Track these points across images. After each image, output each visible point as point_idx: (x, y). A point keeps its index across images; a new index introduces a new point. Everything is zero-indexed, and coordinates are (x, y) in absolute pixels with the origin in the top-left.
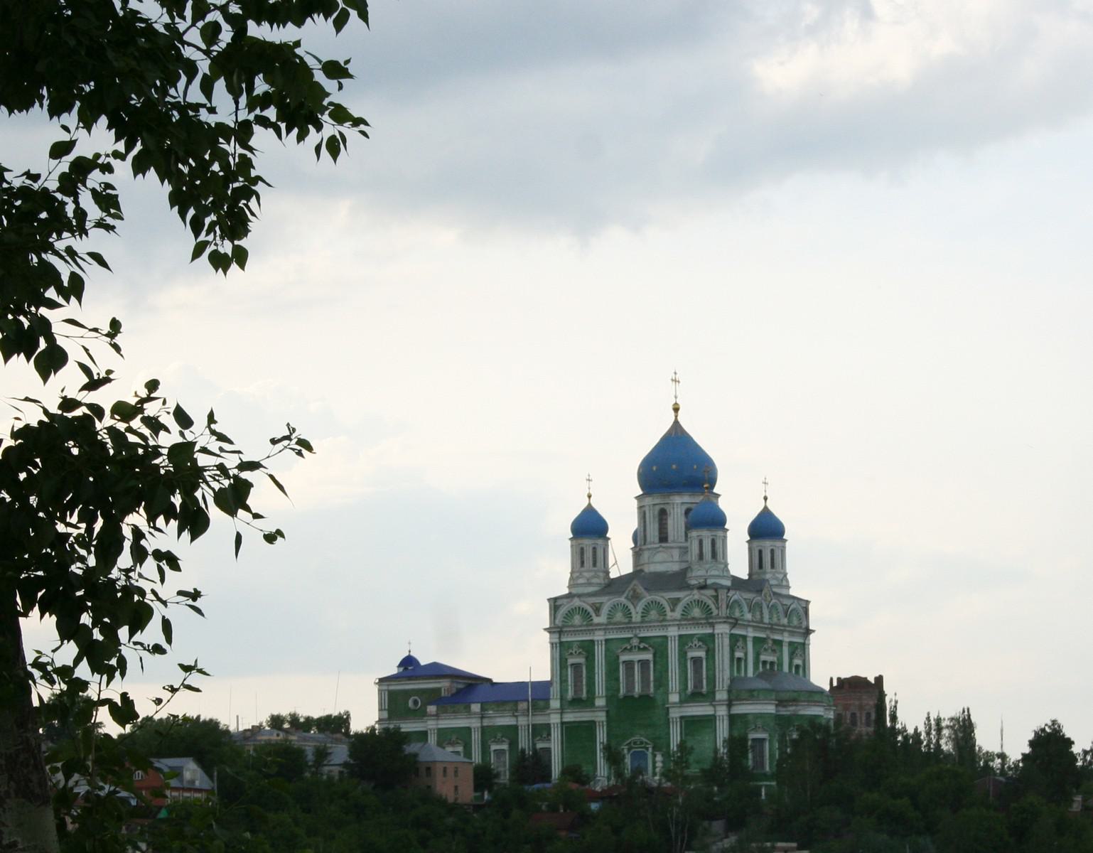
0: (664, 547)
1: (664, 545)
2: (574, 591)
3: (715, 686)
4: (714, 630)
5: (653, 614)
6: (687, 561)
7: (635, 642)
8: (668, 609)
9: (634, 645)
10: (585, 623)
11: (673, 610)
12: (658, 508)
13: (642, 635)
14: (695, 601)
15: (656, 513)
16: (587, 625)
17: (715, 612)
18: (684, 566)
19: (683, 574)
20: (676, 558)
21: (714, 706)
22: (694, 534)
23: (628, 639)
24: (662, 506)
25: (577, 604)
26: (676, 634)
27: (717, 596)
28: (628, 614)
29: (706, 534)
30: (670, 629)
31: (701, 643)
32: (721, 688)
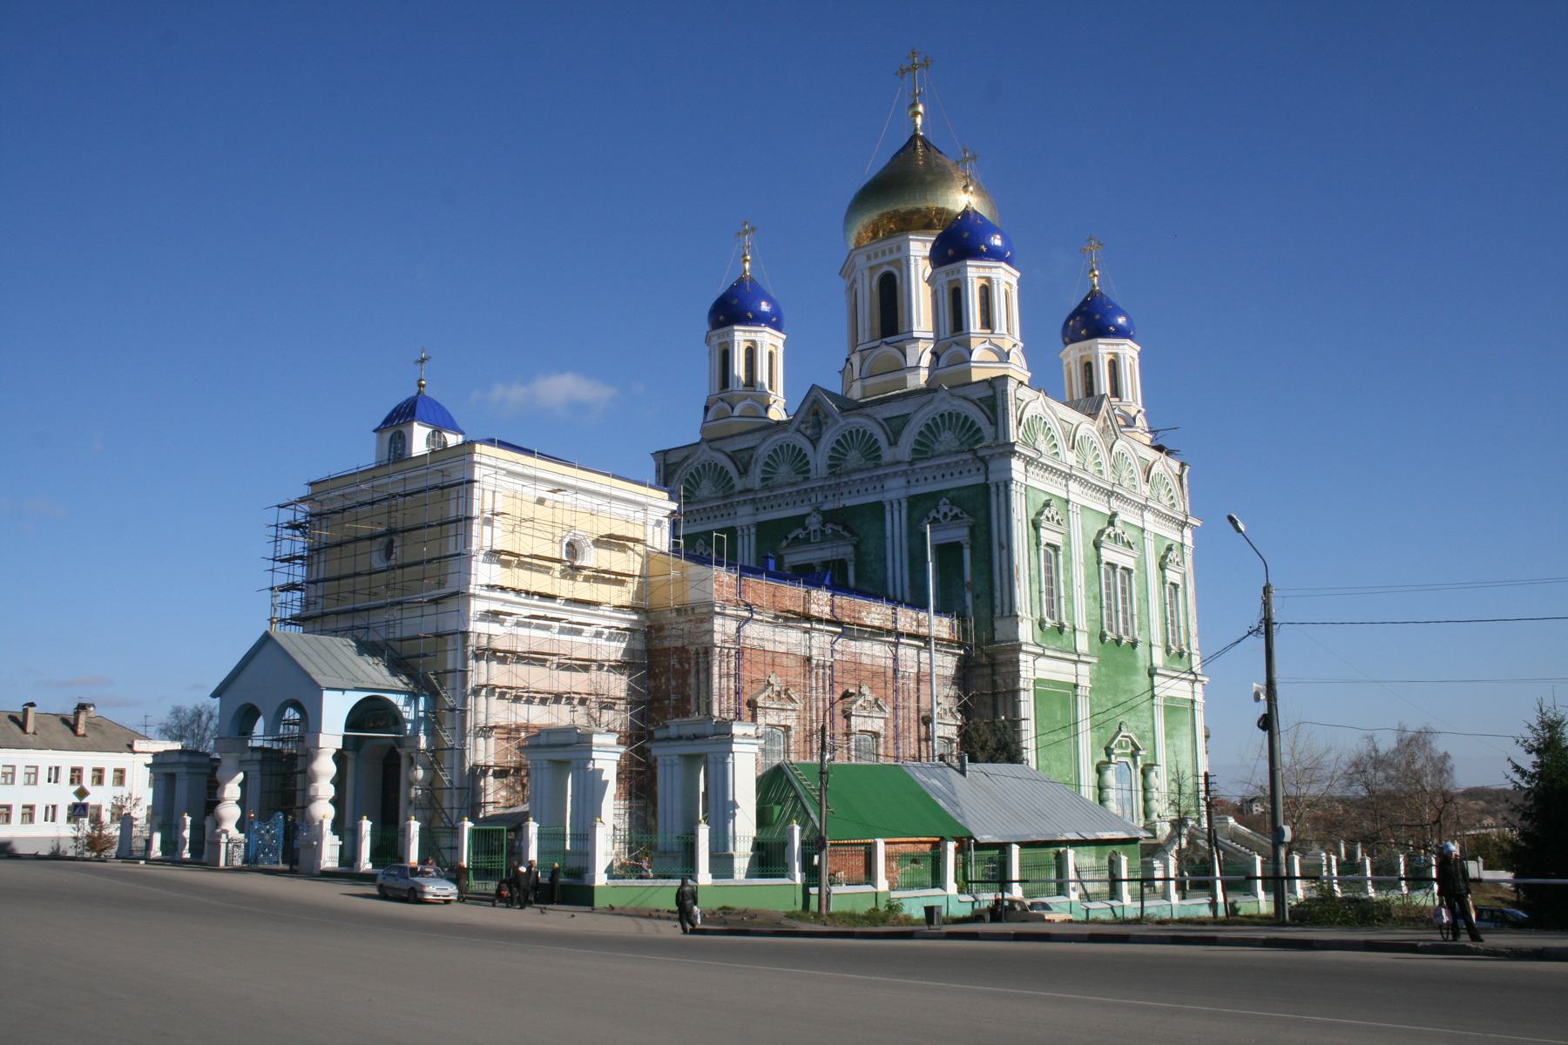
3: (993, 612)
5: (854, 457)
7: (814, 523)
9: (812, 528)
10: (720, 494)
11: (893, 443)
13: (826, 507)
14: (942, 415)
16: (724, 498)
23: (800, 521)
24: (886, 268)
25: (703, 459)
26: (902, 494)
27: (994, 397)
28: (800, 461)
30: (889, 484)
31: (956, 510)
32: (1006, 613)
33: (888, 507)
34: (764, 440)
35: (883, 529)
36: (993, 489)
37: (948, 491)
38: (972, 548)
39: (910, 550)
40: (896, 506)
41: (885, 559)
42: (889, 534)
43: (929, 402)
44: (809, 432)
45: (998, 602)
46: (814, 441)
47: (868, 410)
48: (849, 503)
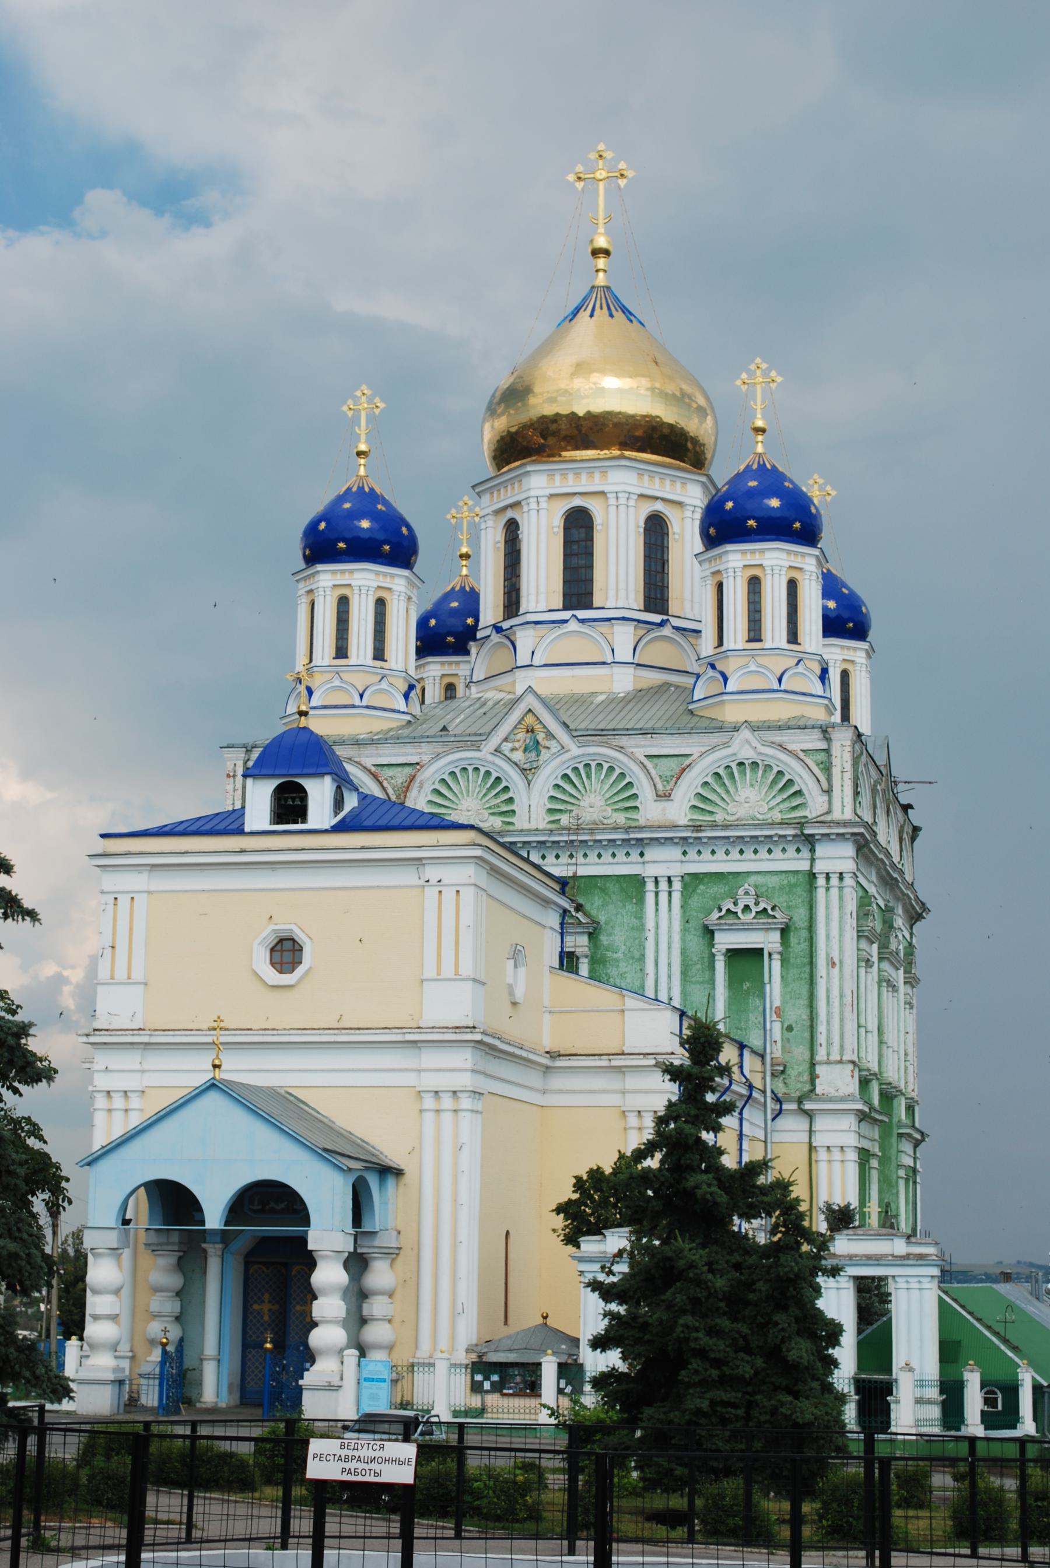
0: (583, 621)
1: (582, 614)
4: (813, 860)
8: (645, 790)
11: (664, 796)
12: (563, 507)
15: (558, 522)
17: (815, 805)
20: (624, 653)
21: (810, 1115)
24: (577, 502)
26: (676, 870)
27: (827, 751)
30: (651, 854)
33: (650, 886)
34: (438, 756)
35: (640, 916)
36: (821, 881)
37: (749, 873)
38: (784, 961)
39: (684, 952)
40: (663, 885)
41: (642, 958)
42: (650, 924)
43: (726, 745)
44: (518, 756)
45: (821, 1038)
46: (527, 772)
47: (624, 741)
48: (582, 871)
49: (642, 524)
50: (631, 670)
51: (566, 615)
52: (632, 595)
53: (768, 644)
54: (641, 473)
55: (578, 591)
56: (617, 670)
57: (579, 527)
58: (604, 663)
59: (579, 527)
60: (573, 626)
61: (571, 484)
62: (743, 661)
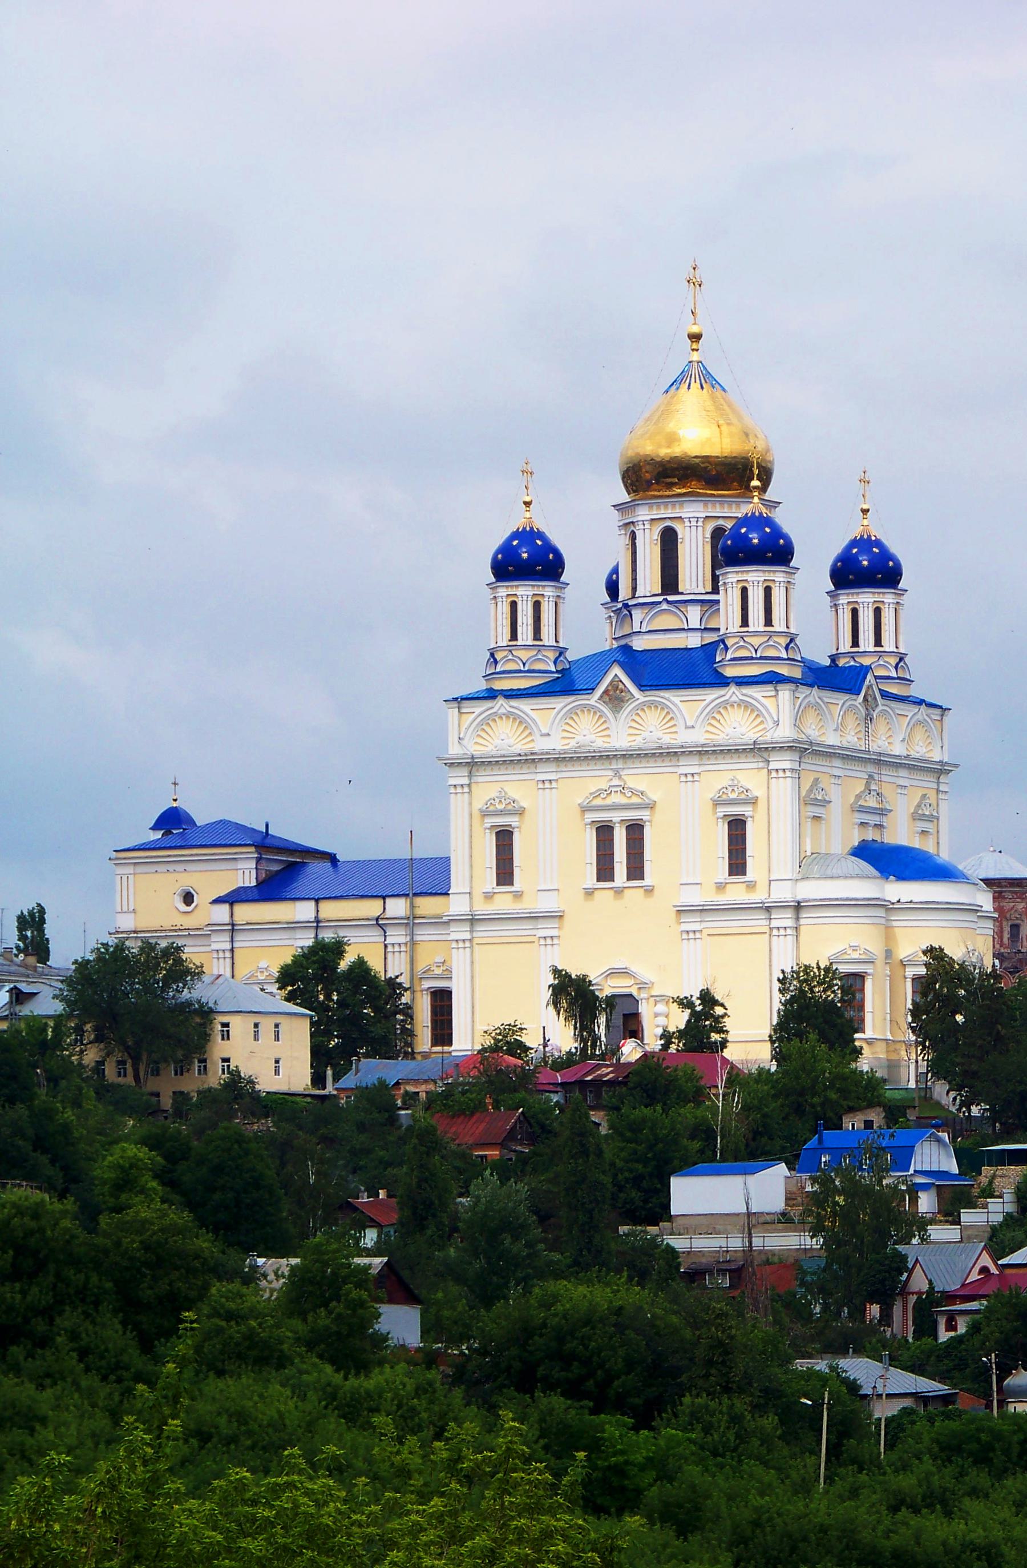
0: (668, 602)
1: (670, 598)
2: (498, 685)
6: (718, 629)
18: (711, 638)
19: (709, 650)
22: (733, 576)
24: (668, 523)
29: (755, 576)
36: (774, 774)
49: (708, 535)
50: (699, 634)
51: (660, 599)
52: (701, 584)
53: (751, 629)
54: (706, 503)
55: (670, 582)
56: (690, 634)
57: (669, 540)
58: (684, 629)
59: (669, 540)
60: (665, 606)
61: (662, 513)
62: (736, 640)
